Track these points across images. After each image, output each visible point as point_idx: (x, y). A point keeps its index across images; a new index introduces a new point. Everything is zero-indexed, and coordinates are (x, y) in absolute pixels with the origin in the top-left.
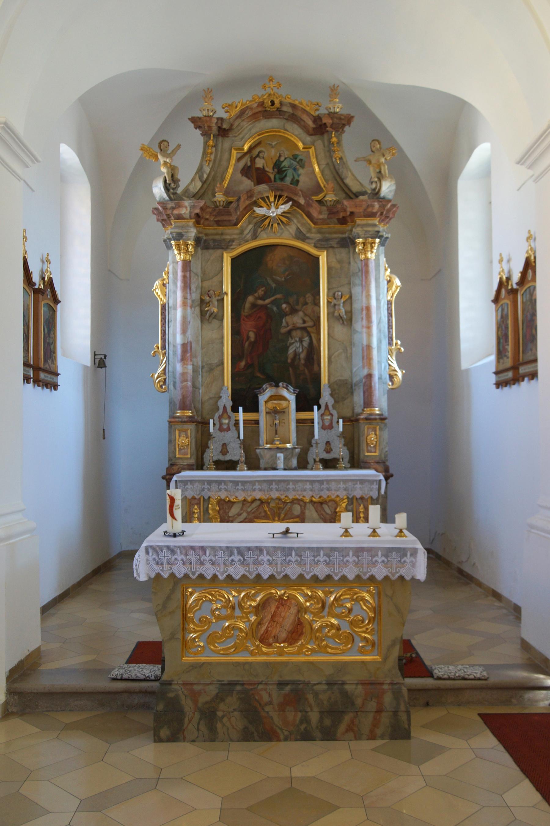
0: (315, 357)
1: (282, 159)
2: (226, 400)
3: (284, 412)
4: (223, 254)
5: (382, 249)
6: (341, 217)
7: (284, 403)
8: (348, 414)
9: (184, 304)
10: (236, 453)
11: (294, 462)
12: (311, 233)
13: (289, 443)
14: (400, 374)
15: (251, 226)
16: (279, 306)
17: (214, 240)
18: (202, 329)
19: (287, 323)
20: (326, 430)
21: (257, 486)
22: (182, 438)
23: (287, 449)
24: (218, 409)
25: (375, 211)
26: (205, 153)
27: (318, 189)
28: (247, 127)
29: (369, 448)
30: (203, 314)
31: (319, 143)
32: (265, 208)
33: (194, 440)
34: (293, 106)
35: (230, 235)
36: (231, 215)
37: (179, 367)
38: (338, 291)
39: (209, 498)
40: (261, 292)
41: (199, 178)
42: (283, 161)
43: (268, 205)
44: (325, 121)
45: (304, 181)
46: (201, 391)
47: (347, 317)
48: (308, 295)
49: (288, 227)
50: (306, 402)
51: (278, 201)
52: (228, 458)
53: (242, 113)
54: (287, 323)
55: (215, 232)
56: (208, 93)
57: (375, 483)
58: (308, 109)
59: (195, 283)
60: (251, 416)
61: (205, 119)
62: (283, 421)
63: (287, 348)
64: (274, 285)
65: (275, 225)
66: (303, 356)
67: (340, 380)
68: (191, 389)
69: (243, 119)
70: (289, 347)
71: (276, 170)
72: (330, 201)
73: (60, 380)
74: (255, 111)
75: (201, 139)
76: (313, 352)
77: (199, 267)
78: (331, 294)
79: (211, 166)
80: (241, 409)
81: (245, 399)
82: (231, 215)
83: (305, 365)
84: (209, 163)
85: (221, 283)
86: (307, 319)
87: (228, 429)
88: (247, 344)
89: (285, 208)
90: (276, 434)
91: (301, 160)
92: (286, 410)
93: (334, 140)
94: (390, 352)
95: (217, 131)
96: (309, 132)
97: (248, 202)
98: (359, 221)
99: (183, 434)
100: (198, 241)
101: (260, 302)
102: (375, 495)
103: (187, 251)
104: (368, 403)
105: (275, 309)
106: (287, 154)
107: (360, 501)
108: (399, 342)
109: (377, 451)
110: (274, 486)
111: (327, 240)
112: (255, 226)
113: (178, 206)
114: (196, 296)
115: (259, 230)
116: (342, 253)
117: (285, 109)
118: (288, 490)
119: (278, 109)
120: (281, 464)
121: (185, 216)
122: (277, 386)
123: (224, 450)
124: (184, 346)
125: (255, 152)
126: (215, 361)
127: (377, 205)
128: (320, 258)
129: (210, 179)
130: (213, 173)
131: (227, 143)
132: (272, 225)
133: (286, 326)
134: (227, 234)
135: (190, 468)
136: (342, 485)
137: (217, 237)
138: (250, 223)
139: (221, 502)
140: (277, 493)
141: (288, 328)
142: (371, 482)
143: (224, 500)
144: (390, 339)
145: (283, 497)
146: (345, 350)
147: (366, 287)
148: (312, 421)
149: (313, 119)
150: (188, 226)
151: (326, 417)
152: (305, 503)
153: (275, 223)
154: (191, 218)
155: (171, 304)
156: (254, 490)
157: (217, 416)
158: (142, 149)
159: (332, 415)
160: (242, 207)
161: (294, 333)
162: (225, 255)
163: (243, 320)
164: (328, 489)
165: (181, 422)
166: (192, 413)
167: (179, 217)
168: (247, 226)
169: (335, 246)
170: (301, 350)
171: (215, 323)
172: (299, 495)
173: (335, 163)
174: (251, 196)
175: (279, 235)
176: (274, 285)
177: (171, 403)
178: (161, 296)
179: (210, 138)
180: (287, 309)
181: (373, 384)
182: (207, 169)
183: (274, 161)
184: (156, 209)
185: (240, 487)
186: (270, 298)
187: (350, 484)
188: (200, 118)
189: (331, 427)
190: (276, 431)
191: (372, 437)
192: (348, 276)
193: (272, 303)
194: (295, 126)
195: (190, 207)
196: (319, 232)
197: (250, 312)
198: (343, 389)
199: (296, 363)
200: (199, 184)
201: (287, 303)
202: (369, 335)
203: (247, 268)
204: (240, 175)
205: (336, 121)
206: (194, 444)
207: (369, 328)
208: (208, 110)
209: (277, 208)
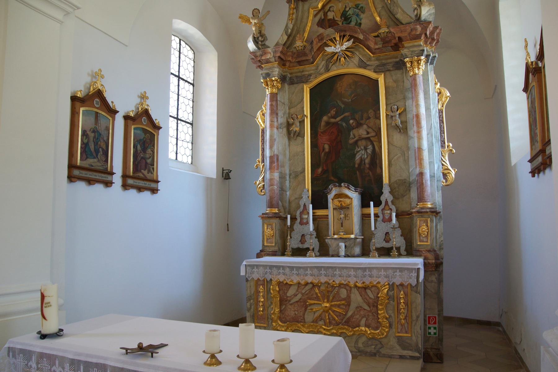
0: (378, 161)
1: (347, 9)
3: (348, 208)
5: (430, 67)
7: (348, 201)
9: (272, 126)
11: (357, 250)
14: (453, 173)
15: (324, 62)
16: (347, 122)
17: (297, 77)
18: (289, 145)
19: (354, 135)
21: (309, 272)
22: (269, 230)
24: (300, 207)
25: (418, 33)
26: (289, 15)
27: (377, 27)
29: (421, 238)
30: (289, 132)
32: (333, 47)
33: (277, 232)
35: (308, 71)
36: (307, 56)
39: (271, 280)
40: (333, 112)
45: (365, 22)
46: (288, 193)
47: (404, 126)
48: (371, 111)
52: (305, 246)
54: (354, 135)
57: (414, 271)
63: (355, 155)
64: (343, 106)
66: (367, 161)
67: (399, 180)
70: (356, 154)
71: (343, 18)
73: (160, 186)
76: (376, 158)
77: (287, 97)
82: (307, 56)
83: (370, 169)
86: (370, 130)
90: (342, 226)
91: (362, 7)
97: (319, 44)
98: (406, 44)
99: (270, 227)
100: (283, 79)
101: (333, 120)
102: (414, 283)
103: (273, 86)
104: (421, 198)
105: (344, 124)
106: (351, 5)
107: (400, 288)
108: (451, 145)
109: (429, 241)
110: (323, 272)
111: (384, 65)
113: (265, 53)
114: (282, 119)
116: (398, 74)
118: (335, 275)
121: (271, 60)
122: (340, 186)
124: (271, 158)
125: (327, 8)
126: (300, 169)
127: (419, 28)
129: (294, 33)
132: (340, 59)
133: (353, 137)
134: (306, 71)
135: (274, 254)
136: (383, 273)
137: (299, 74)
139: (280, 284)
140: (325, 278)
142: (410, 270)
143: (282, 282)
144: (443, 142)
145: (331, 282)
146: (403, 154)
147: (415, 97)
150: (274, 67)
151: (386, 212)
152: (351, 287)
153: (343, 58)
154: (276, 61)
156: (306, 275)
157: (298, 212)
158: (240, 18)
159: (391, 209)
160: (315, 48)
161: (360, 143)
162: (305, 86)
164: (371, 276)
165: (268, 217)
166: (278, 210)
167: (268, 61)
169: (391, 69)
170: (366, 156)
171: (299, 139)
172: (345, 281)
173: (388, 4)
174: (322, 39)
175: (345, 66)
176: (343, 106)
178: (262, 123)
181: (424, 181)
182: (291, 26)
184: (252, 59)
185: (295, 272)
187: (390, 271)
190: (342, 224)
191: (424, 228)
192: (404, 91)
193: (341, 120)
199: (362, 167)
200: (285, 37)
201: (354, 119)
202: (420, 138)
203: (322, 95)
206: (277, 235)
209: (342, 45)
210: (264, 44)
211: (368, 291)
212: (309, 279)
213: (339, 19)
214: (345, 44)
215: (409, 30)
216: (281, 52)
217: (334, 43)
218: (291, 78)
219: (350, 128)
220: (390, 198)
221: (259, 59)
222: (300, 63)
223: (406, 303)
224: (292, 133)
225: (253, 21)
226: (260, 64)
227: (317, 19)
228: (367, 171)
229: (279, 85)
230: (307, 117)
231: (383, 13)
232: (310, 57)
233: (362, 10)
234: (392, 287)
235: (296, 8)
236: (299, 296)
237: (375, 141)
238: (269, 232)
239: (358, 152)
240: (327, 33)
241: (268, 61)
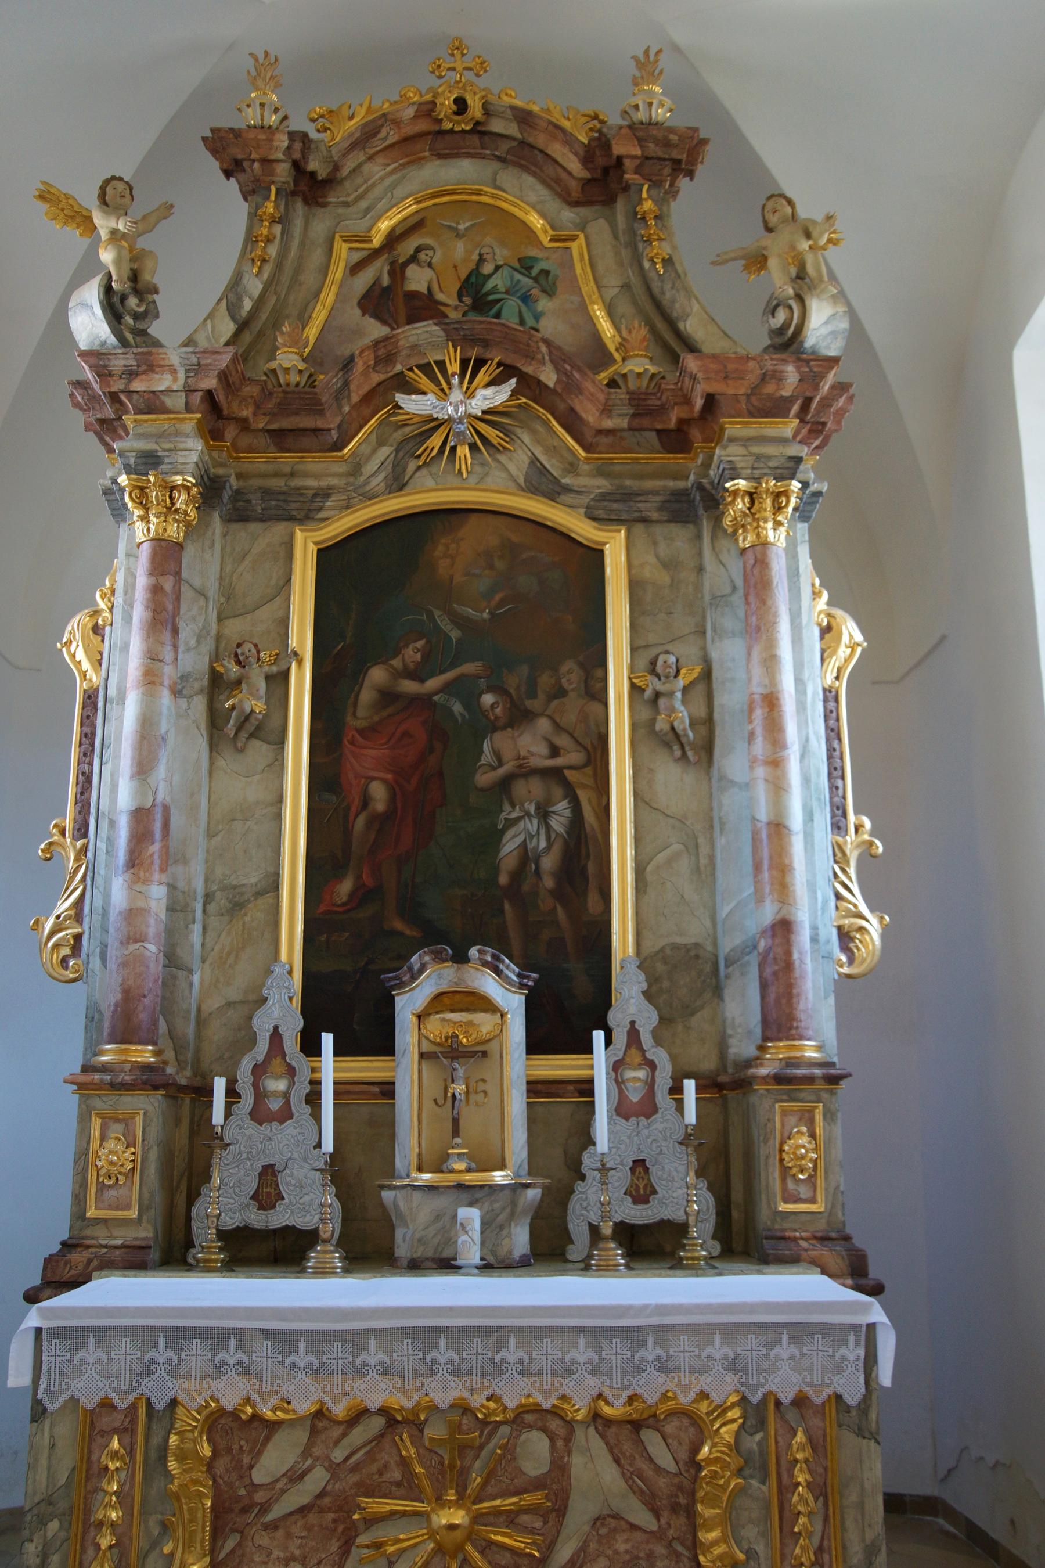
0: (591, 868)
1: (487, 269)
2: (283, 1009)
4: (292, 536)
5: (802, 528)
6: (672, 424)
7: (485, 1022)
8: (708, 1064)
9: (150, 678)
10: (309, 1203)
11: (520, 1239)
12: (578, 475)
13: (502, 1167)
14: (873, 926)
15: (385, 451)
16: (471, 701)
17: (267, 493)
18: (210, 773)
19: (498, 755)
20: (633, 1120)
21: (374, 1356)
22: (111, 1144)
23: (493, 1189)
24: (253, 1040)
25: (786, 393)
26: (251, 240)
28: (382, 179)
29: (791, 1185)
30: (215, 720)
31: (600, 228)
32: (431, 397)
33: (153, 1155)
34: (524, 117)
35: (317, 476)
36: (321, 413)
37: (119, 892)
38: (667, 652)
39: (174, 1403)
40: (412, 654)
41: (228, 309)
42: (490, 276)
43: (442, 390)
44: (618, 149)
46: (196, 978)
49: (502, 458)
50: (563, 1018)
51: (470, 382)
52: (278, 1218)
53: (369, 133)
54: (498, 755)
55: (270, 468)
56: (265, 69)
57: (852, 1339)
58: (566, 124)
59: (195, 620)
60: (366, 1068)
61: (251, 135)
62: (482, 1086)
63: (495, 837)
64: (455, 634)
65: (463, 451)
66: (548, 863)
67: (675, 947)
68: (155, 968)
69: (371, 151)
70: (503, 832)
71: (468, 300)
72: (639, 375)
74: (409, 130)
75: (241, 209)
77: (214, 570)
78: (643, 663)
79: (265, 276)
80: (328, 1040)
81: (349, 1005)
82: (321, 413)
83: (558, 894)
84: (260, 268)
85: (284, 623)
87: (285, 1115)
88: (360, 823)
89: (498, 396)
90: (456, 1132)
91: (547, 273)
92: (493, 1047)
93: (648, 205)
94: (839, 855)
95: (289, 176)
96: (569, 194)
97: (376, 378)
98: (733, 427)
99: (116, 1130)
100: (210, 490)
101: (409, 686)
102: (853, 1392)
103: (171, 509)
104: (780, 1020)
105: (457, 708)
106: (502, 254)
107: (792, 1416)
108: (867, 824)
109: (820, 1196)
110: (443, 1354)
111: (628, 496)
112: (397, 451)
113: (149, 366)
114: (194, 660)
115: (412, 465)
116: (677, 540)
117: (497, 126)
118: (500, 1369)
119: (478, 130)
120: (470, 1249)
121: (169, 402)
122: (461, 958)
123: (267, 1190)
124: (140, 816)
126: (253, 878)
127: (791, 374)
128: (607, 549)
129: (264, 316)
130: (272, 301)
131: (321, 224)
132: (454, 449)
133: (495, 763)
134: (306, 475)
135: (134, 1260)
136: (718, 1349)
137: (278, 483)
138: (381, 443)
139: (220, 1423)
140: (454, 1382)
141: (501, 771)
142: (835, 1333)
143: (234, 1415)
144: (839, 812)
145: (477, 1400)
146: (692, 846)
147: (759, 628)
148: (586, 1087)
149: (582, 153)
150: (178, 434)
151: (630, 1074)
152: (570, 1425)
153: (464, 447)
154: (188, 409)
155: (112, 692)
156: (360, 1372)
157: (246, 1065)
159: (652, 1065)
160: (360, 385)
161: (520, 788)
162: (299, 535)
163: (352, 742)
164: (664, 1368)
165: (113, 1086)
166: (157, 1053)
167: (152, 405)
168: (374, 451)
169: (655, 515)
170: (543, 844)
171: (259, 751)
172: (547, 1394)
174: (389, 359)
175: (473, 481)
176: (455, 634)
177: (93, 1017)
178: (86, 665)
179: (268, 198)
180: (498, 711)
181: (795, 956)
182: (254, 286)
183: (463, 277)
184: (81, 385)
185: (302, 1358)
186: (442, 672)
187: (752, 1340)
188: (236, 133)
189: (648, 1108)
190: (456, 1122)
193: (446, 688)
194: (529, 180)
195: (187, 371)
196: (601, 472)
197: (376, 718)
198: (687, 977)
199: (526, 887)
200: (227, 328)
202: (778, 787)
203: (370, 581)
204: (358, 312)
205: (653, 149)
206: (152, 1168)
207: (776, 763)
208: (262, 105)
209: (470, 394)
210: (144, 333)
211: (651, 1438)
212: (377, 1393)
213: (453, 301)
214: (481, 393)
215: (752, 378)
216: (223, 376)
217: (438, 384)
218: (238, 492)
219: (483, 726)
220: (648, 1019)
221: (117, 386)
222: (282, 439)
223: (820, 1490)
224: (231, 721)
225: (103, 223)
226: (109, 412)
227: (363, 281)
228: (546, 903)
229: (193, 514)
230: (300, 662)
231: (624, 307)
232: (331, 421)
233: (547, 283)
234: (758, 1413)
235: (283, 220)
236: (317, 1479)
237: (584, 786)
238: (113, 1153)
239: (512, 823)
240: (413, 340)
241: (152, 405)
